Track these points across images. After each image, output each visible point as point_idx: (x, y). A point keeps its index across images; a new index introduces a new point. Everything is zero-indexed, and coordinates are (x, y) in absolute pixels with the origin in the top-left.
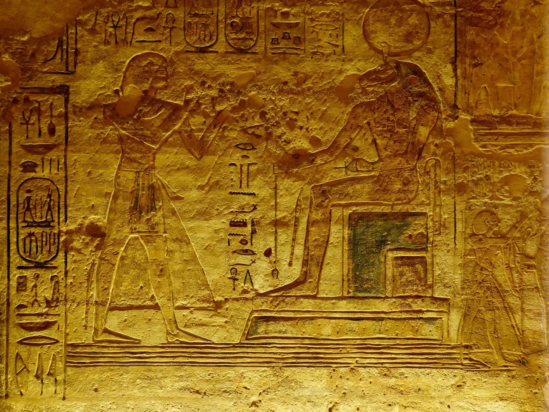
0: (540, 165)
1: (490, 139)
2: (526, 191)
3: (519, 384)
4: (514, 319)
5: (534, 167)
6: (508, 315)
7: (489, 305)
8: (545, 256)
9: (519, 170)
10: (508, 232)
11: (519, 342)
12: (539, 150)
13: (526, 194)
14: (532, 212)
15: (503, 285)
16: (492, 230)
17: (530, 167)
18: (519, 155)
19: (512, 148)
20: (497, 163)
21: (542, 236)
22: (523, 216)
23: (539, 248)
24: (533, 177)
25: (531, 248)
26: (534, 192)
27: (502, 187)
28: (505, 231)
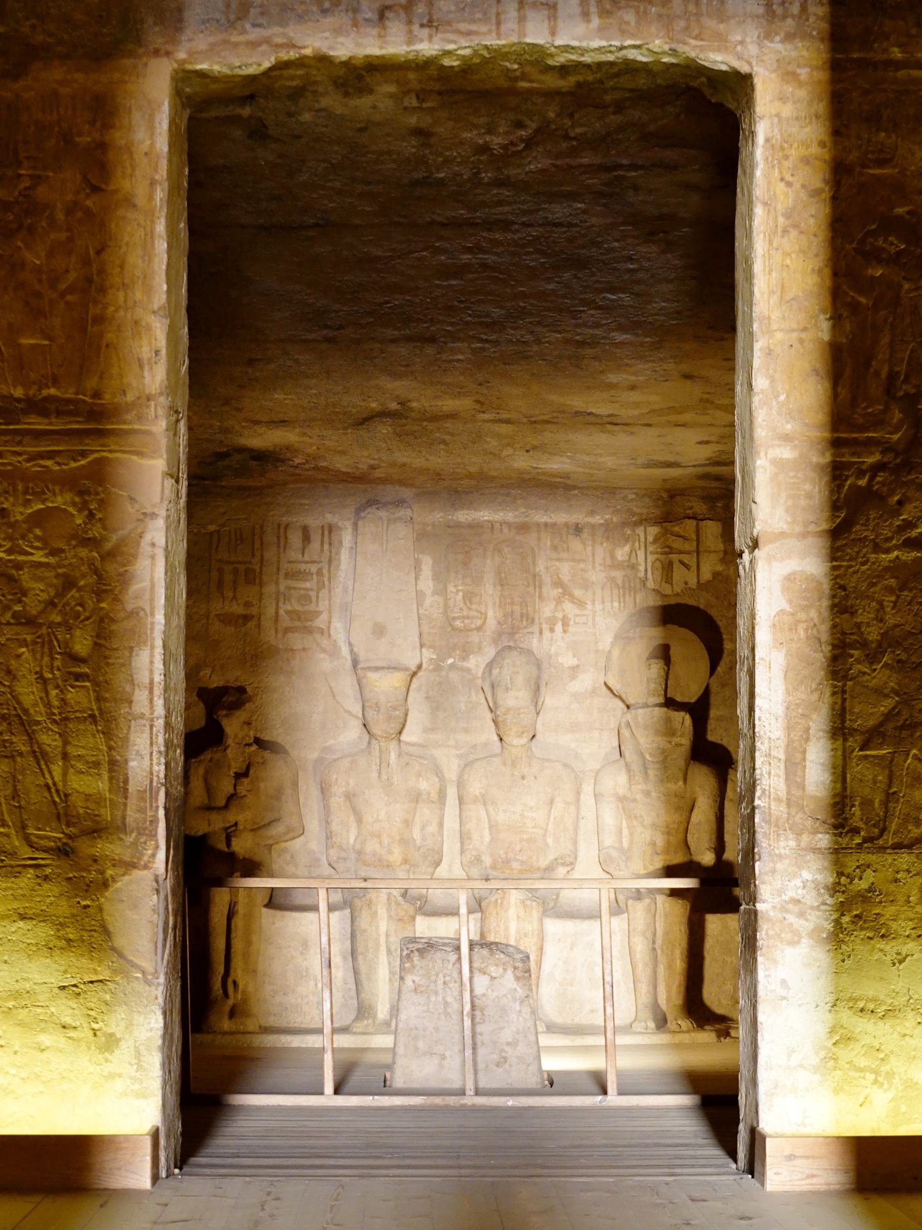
0: (100, 489)
1: (6, 441)
2: (73, 537)
3: (56, 890)
4: (50, 772)
5: (88, 492)
6: (38, 763)
7: (6, 747)
8: (106, 657)
9: (61, 500)
10: (42, 612)
11: (59, 814)
12: (100, 462)
13: (74, 543)
14: (84, 576)
15: (32, 711)
16: (9, 608)
17: (81, 493)
18: (62, 471)
19: (49, 458)
20: (20, 487)
21: (102, 620)
22: (69, 583)
23: (96, 644)
24: (86, 513)
25: (82, 645)
26: (89, 539)
27: (30, 530)
28: (34, 612)
